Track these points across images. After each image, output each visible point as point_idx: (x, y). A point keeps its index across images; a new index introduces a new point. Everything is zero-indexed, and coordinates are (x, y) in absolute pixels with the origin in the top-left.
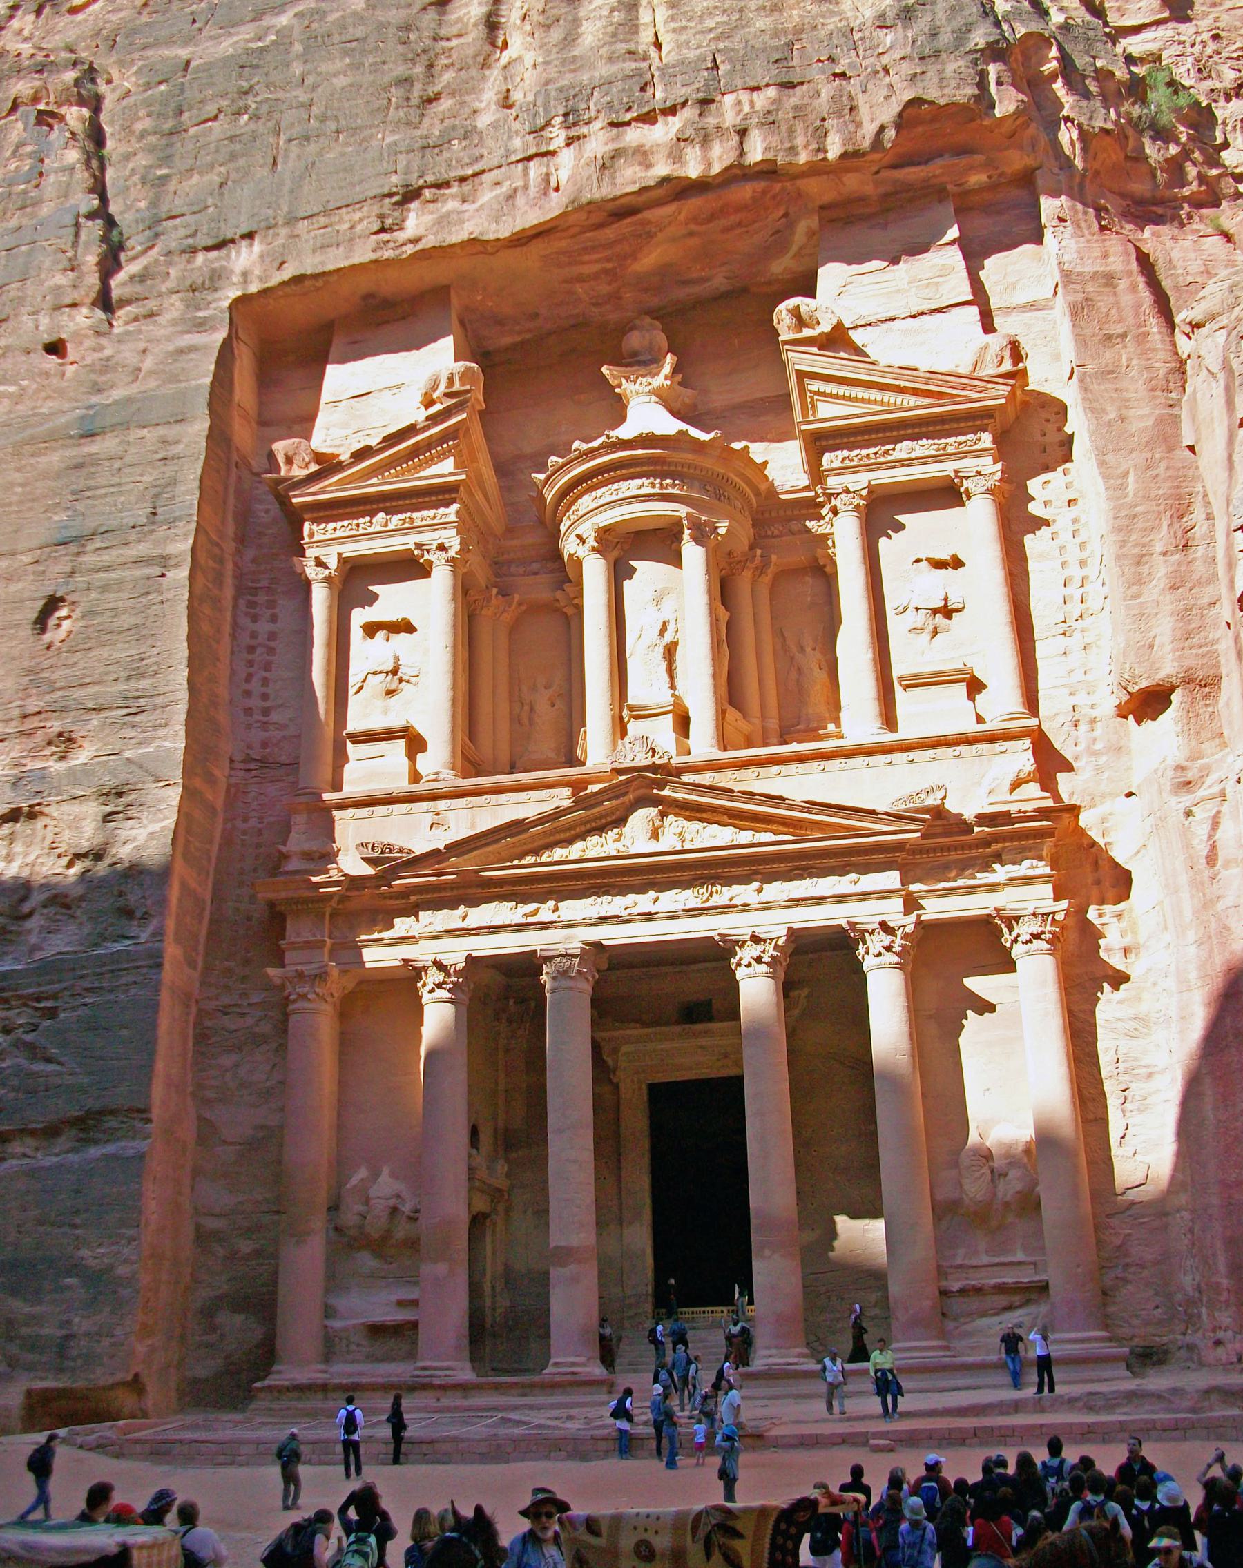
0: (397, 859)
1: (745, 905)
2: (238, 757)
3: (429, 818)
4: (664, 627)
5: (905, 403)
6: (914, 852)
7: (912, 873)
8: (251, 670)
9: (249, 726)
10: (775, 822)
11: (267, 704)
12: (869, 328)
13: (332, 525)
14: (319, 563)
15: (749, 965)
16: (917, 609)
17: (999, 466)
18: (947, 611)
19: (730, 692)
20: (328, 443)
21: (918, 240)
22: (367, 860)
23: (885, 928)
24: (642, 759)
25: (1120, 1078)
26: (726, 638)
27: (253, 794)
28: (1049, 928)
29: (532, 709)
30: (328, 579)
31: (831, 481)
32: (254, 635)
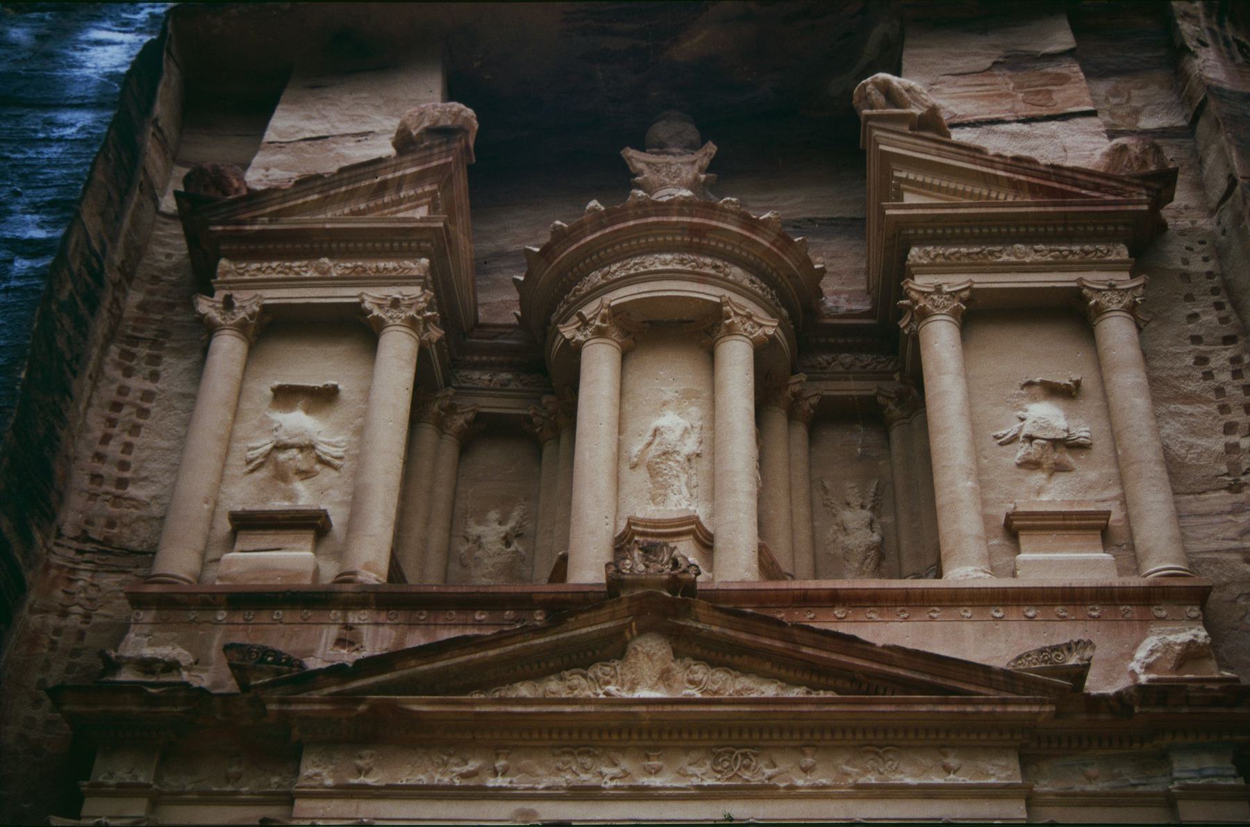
0: (279, 673)
1: (792, 787)
2: (68, 530)
3: (332, 632)
4: (686, 431)
5: (1018, 200)
8: (110, 431)
9: (94, 496)
11: (127, 475)
13: (255, 266)
14: (228, 304)
16: (1030, 438)
21: (1025, 48)
27: (81, 583)
29: (480, 547)
32: (123, 391)
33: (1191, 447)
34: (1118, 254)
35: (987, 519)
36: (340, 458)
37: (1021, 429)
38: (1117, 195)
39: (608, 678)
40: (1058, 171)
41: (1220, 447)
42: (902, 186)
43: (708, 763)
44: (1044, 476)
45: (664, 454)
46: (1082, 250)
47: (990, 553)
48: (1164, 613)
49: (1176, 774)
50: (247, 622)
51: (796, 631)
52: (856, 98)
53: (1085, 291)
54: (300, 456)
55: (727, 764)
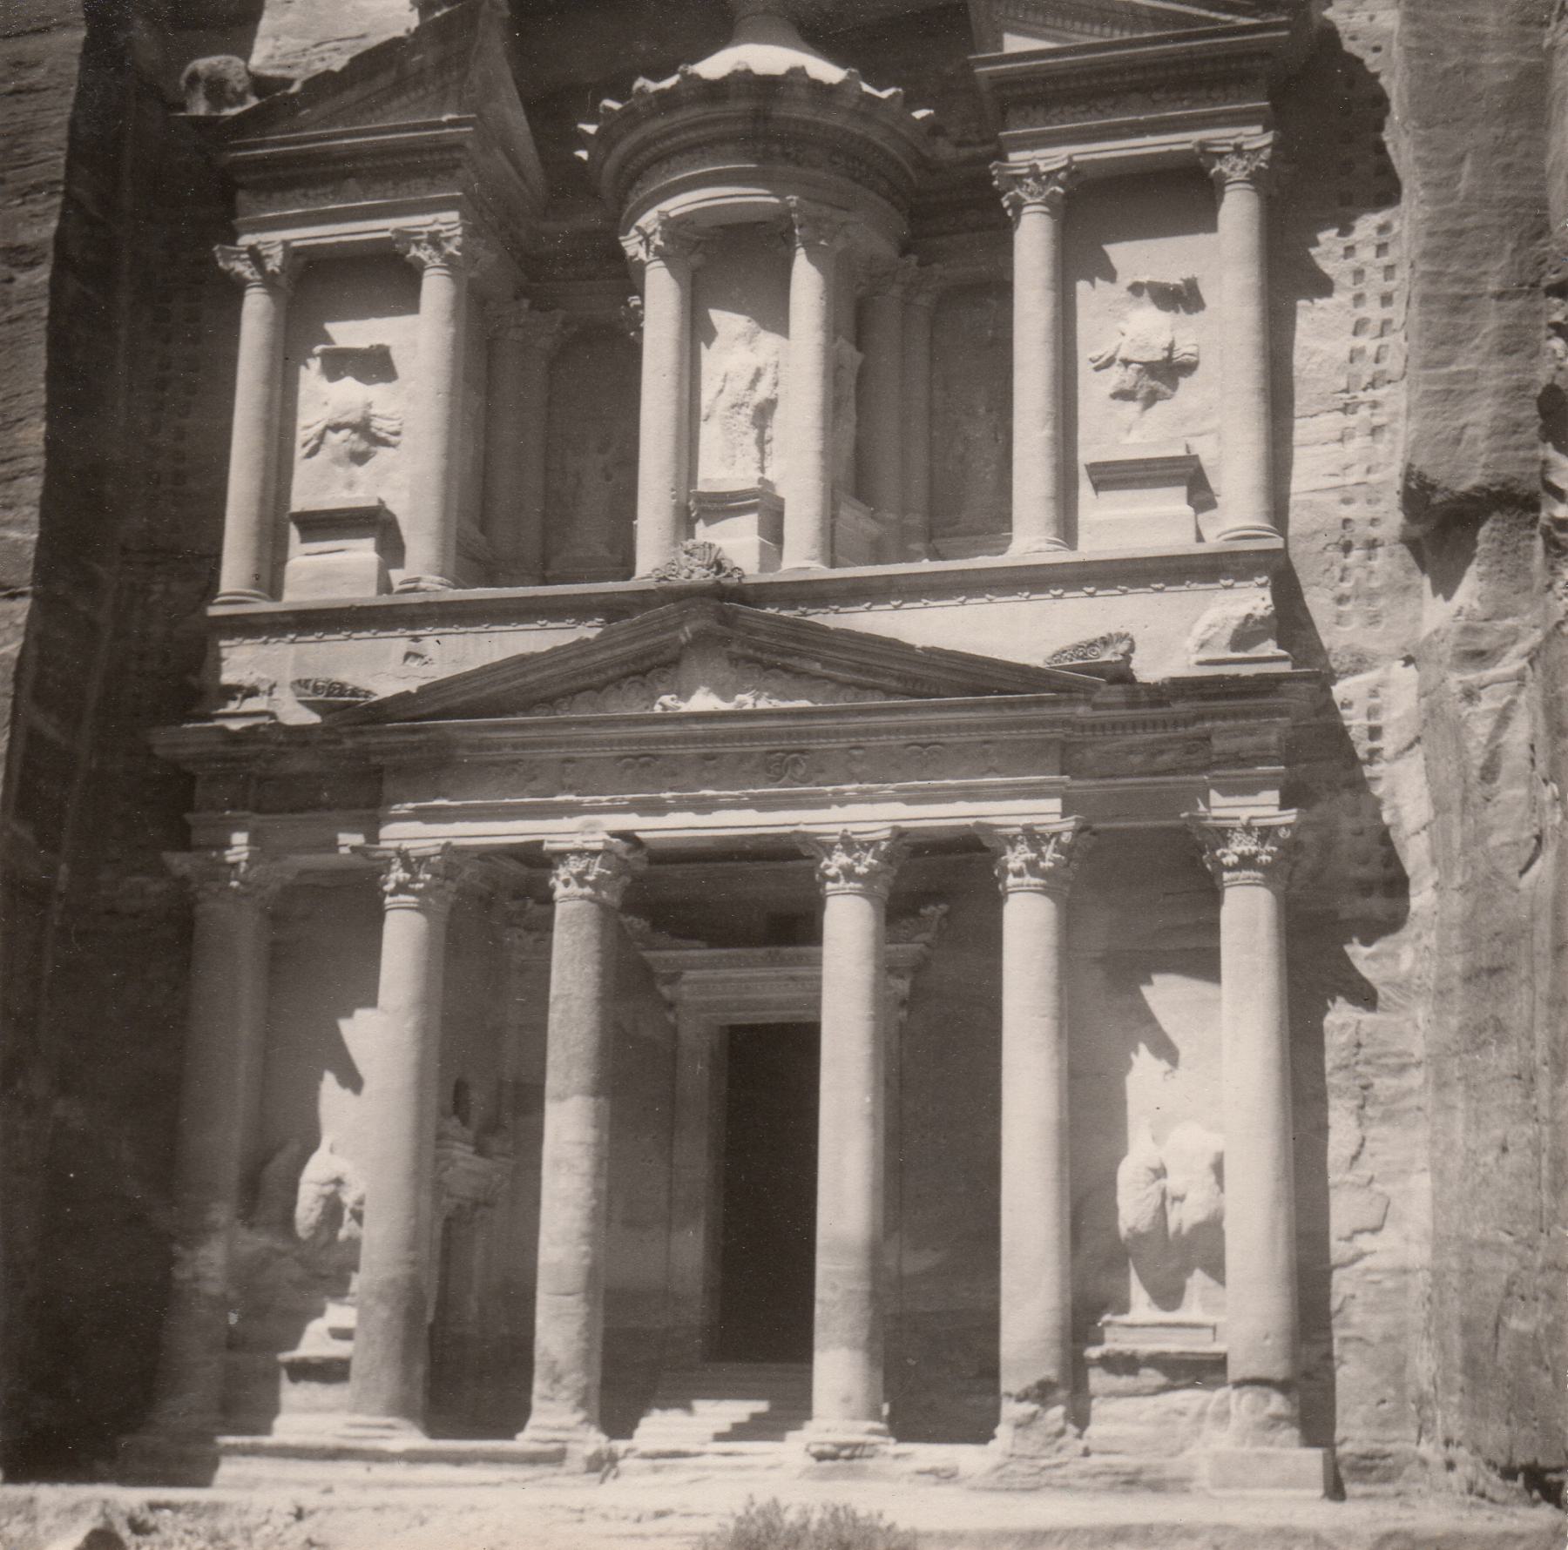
0: (348, 705)
6: (1083, 728)
7: (1078, 756)
10: (885, 676)
15: (835, 879)
16: (1126, 363)
17: (1268, 139)
18: (1168, 371)
19: (853, 476)
20: (276, 61)
22: (310, 705)
23: (1033, 837)
24: (701, 576)
25: (1360, 1069)
26: (852, 392)
28: (1268, 848)
30: (270, 282)
33: (1313, 353)
36: (397, 434)
37: (1118, 350)
41: (1344, 355)
45: (733, 406)
50: (320, 640)
54: (355, 437)
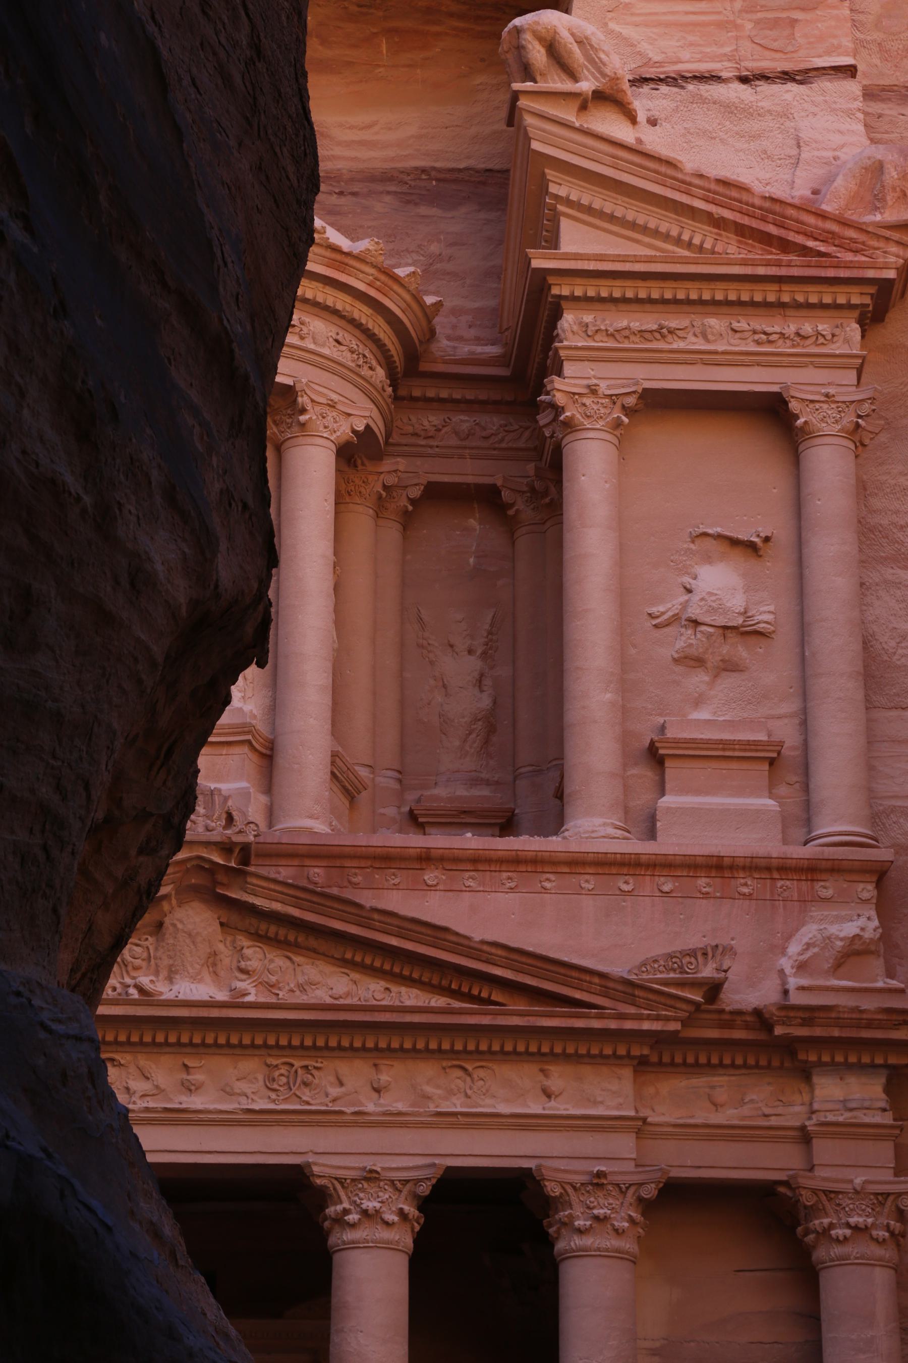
7: (652, 1090)
12: (664, 89)
16: (696, 623)
31: (569, 369)
34: (847, 341)
35: (625, 738)
38: (856, 252)
39: (138, 962)
40: (777, 208)
42: (560, 208)
43: (260, 1077)
44: (706, 678)
46: (798, 334)
47: (626, 788)
48: (829, 893)
49: (816, 1106)
51: (376, 916)
52: (504, 46)
53: (794, 406)
55: (284, 1080)
